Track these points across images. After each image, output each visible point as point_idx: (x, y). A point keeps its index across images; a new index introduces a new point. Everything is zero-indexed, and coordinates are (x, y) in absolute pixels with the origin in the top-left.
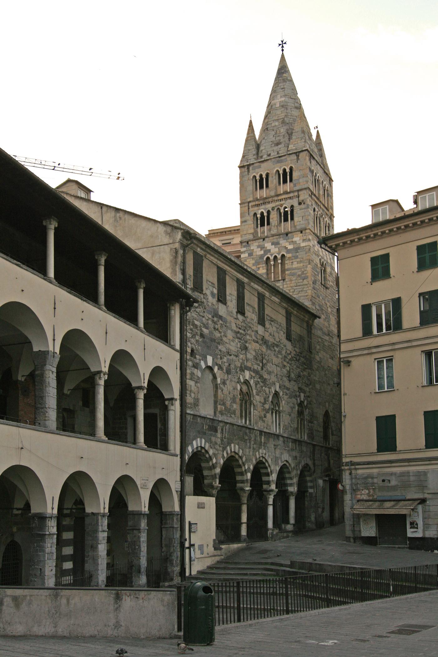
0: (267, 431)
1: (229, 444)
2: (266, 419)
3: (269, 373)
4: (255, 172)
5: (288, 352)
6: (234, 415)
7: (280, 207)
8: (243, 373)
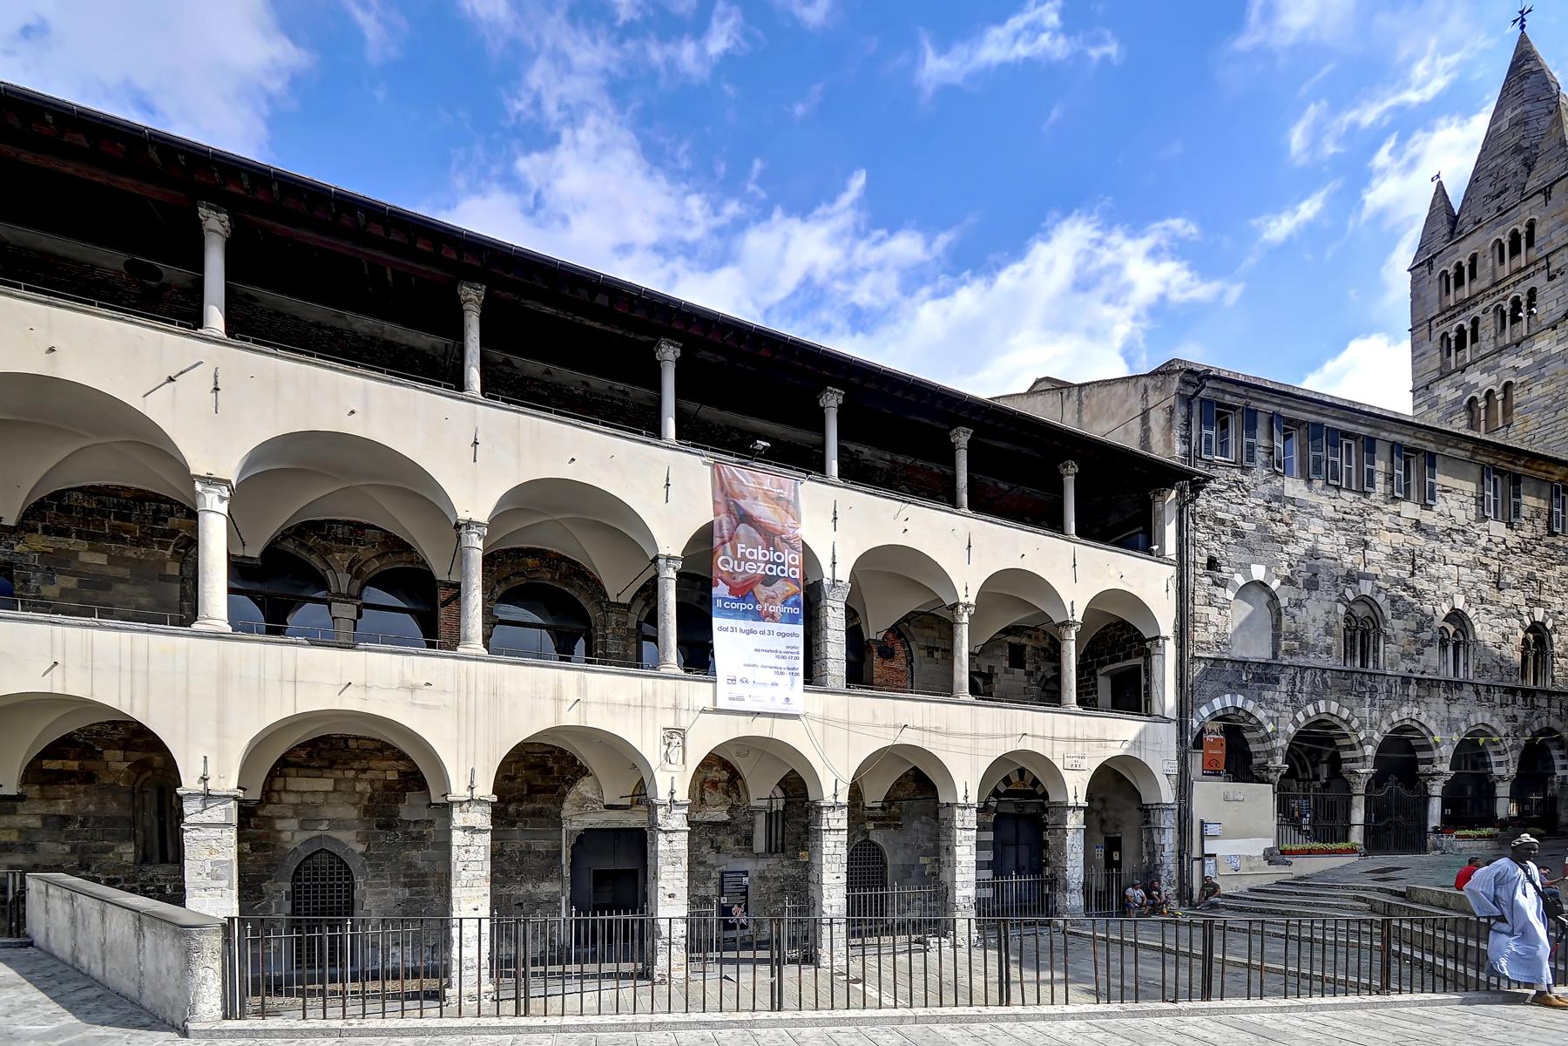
3: (1435, 579)
8: (1354, 585)
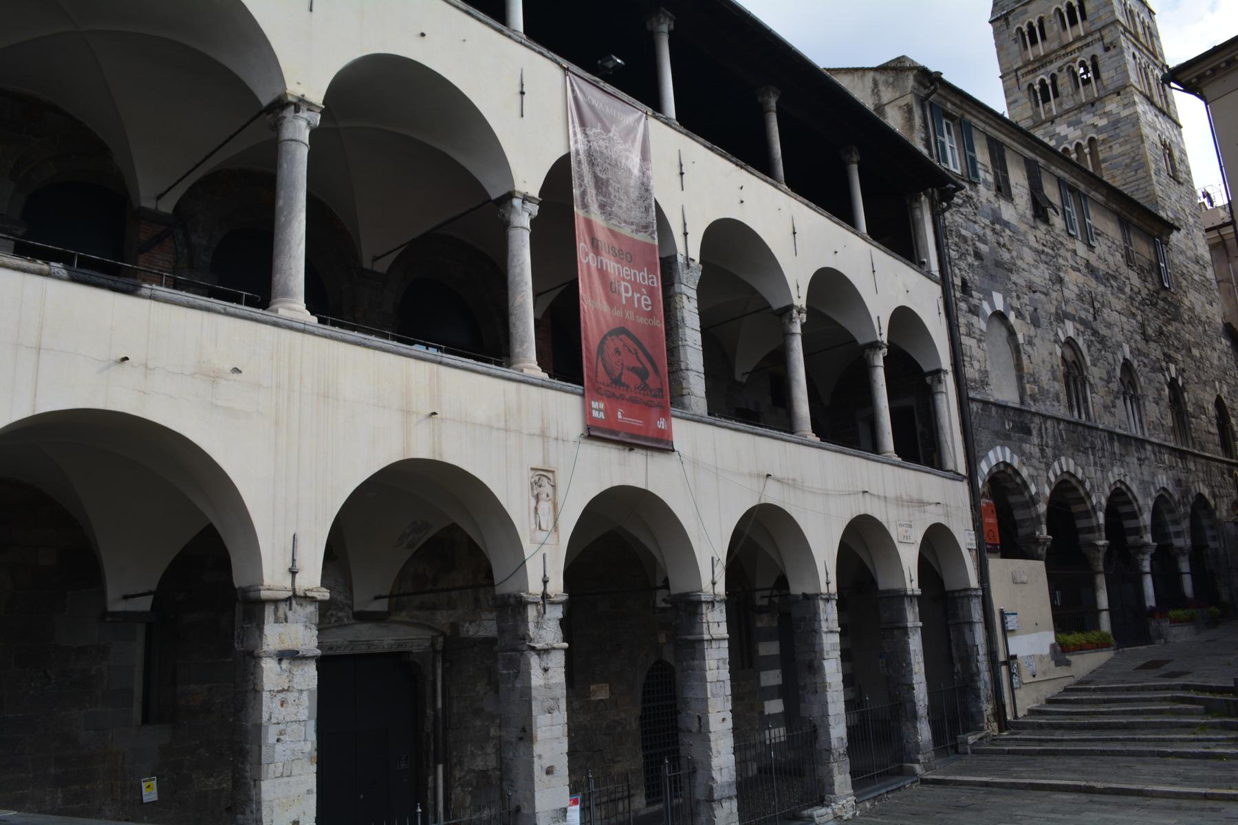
0: (1120, 431)
1: (1056, 457)
2: (1116, 411)
3: (1109, 326)
4: (1018, 22)
5: (1136, 290)
6: (1059, 401)
7: (1072, 64)
8: (1061, 325)
